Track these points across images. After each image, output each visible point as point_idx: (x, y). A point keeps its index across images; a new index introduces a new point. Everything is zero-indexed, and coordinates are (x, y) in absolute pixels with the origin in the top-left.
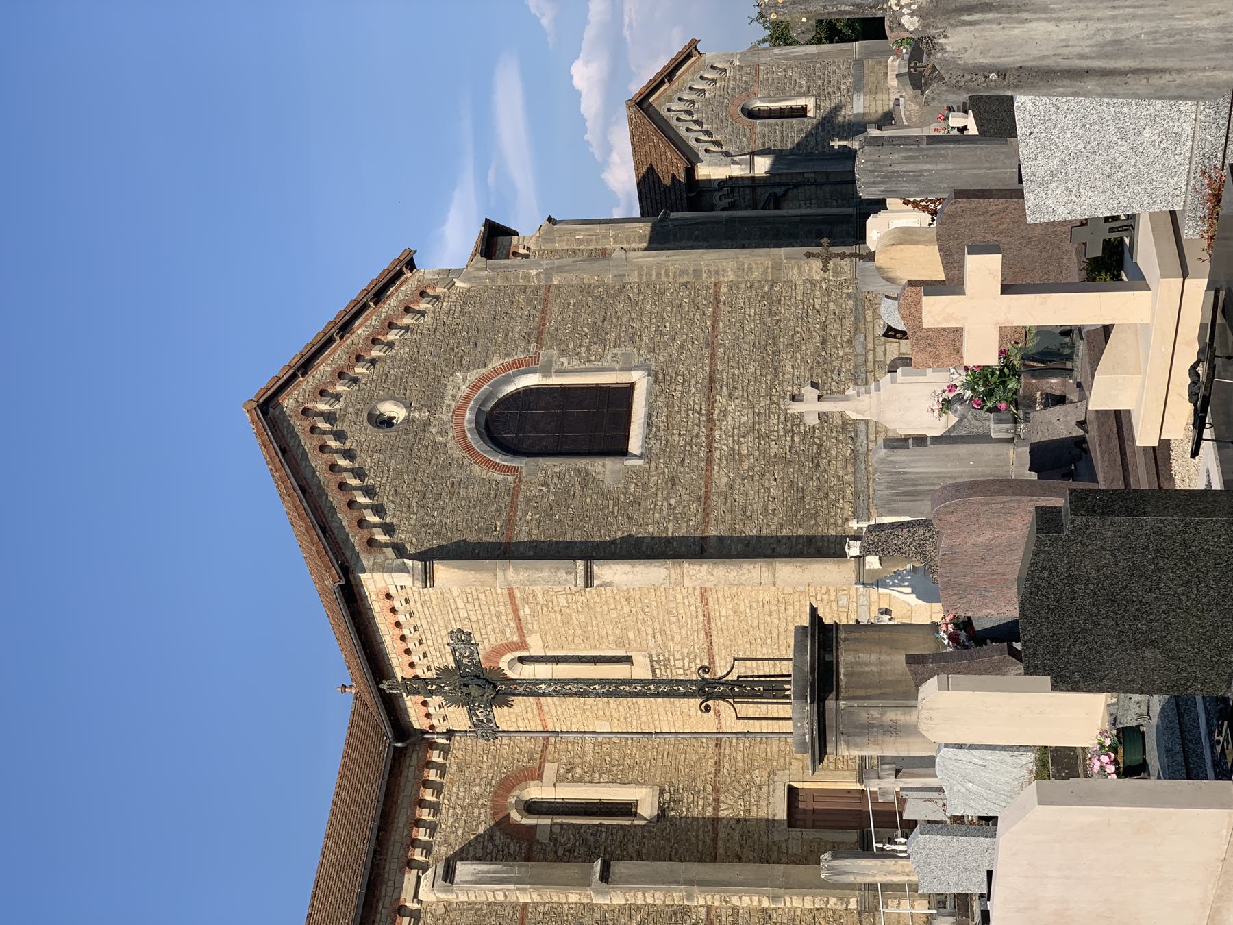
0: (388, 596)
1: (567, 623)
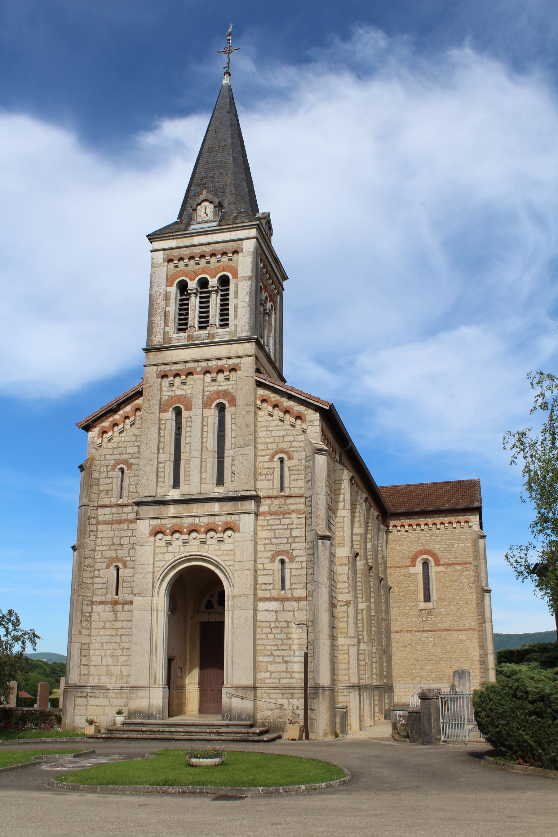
1: (453, 581)
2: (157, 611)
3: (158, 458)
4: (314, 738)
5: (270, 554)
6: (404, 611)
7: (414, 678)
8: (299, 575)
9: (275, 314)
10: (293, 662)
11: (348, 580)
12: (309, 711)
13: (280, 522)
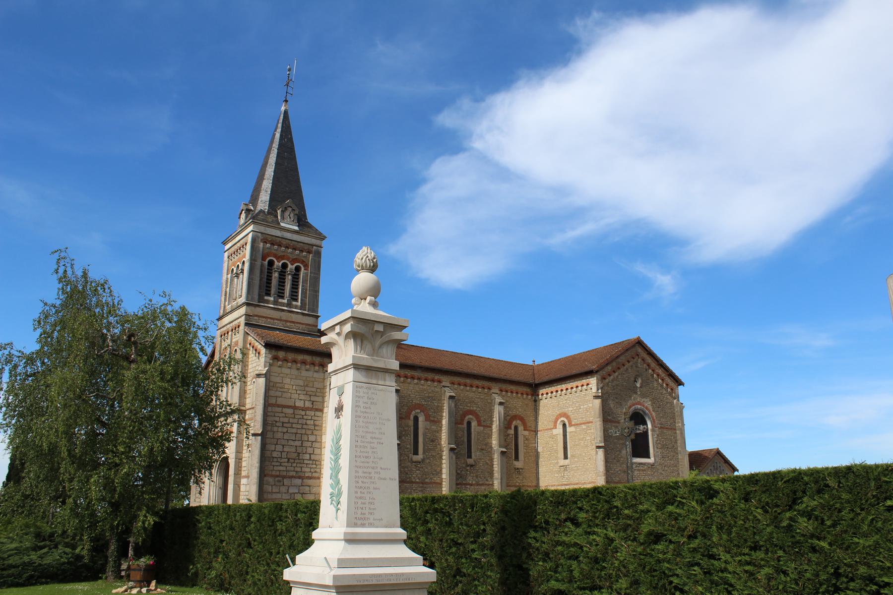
0: (588, 384)
1: (579, 440)
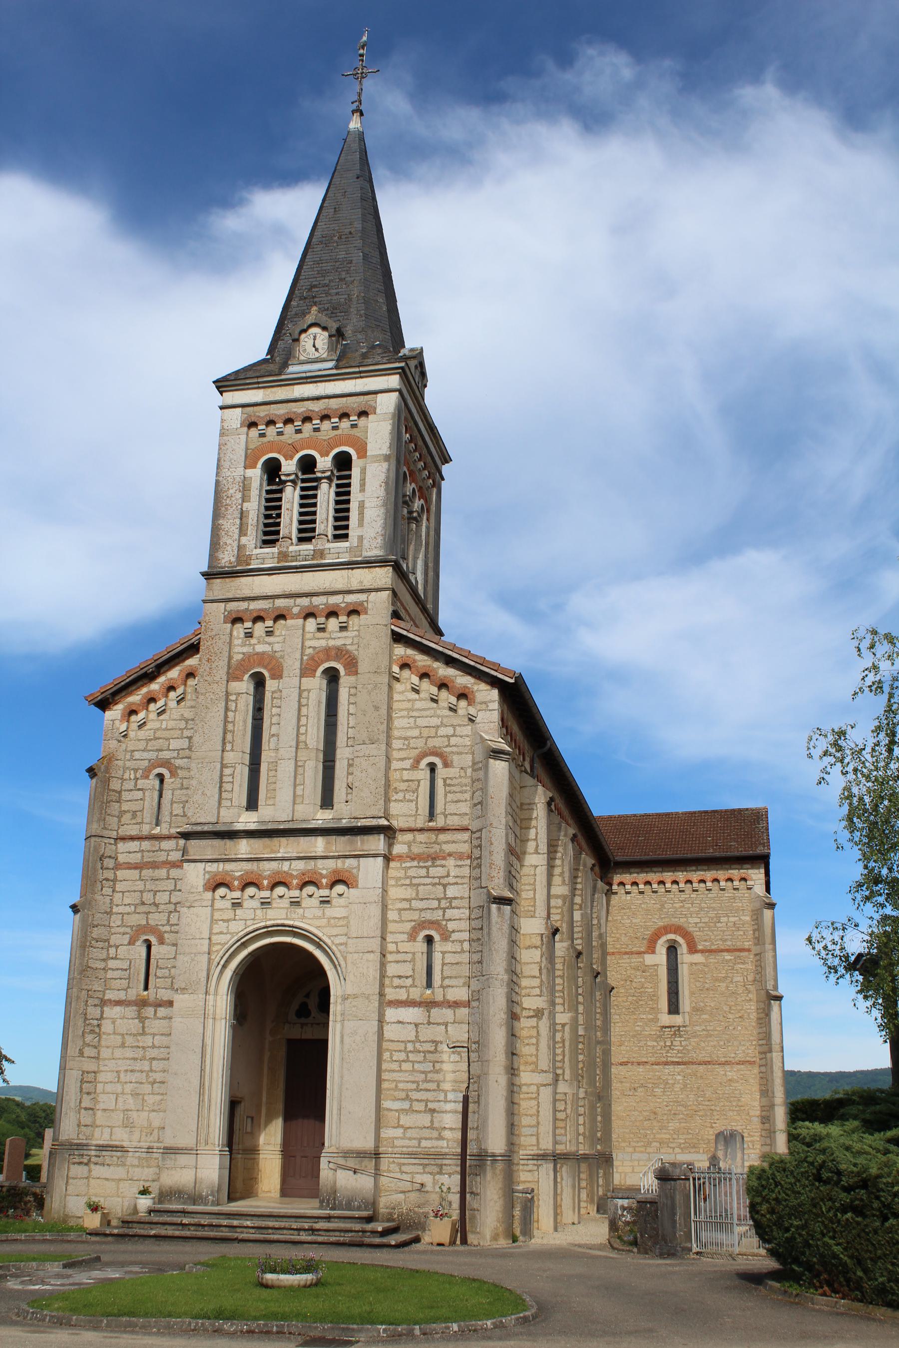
2: (214, 1019)
3: (222, 758)
4: (476, 1243)
5: (408, 926)
6: (634, 1028)
7: (649, 1144)
8: (457, 963)
9: (428, 520)
10: (443, 1112)
11: (541, 974)
12: (468, 1196)
13: (428, 872)
